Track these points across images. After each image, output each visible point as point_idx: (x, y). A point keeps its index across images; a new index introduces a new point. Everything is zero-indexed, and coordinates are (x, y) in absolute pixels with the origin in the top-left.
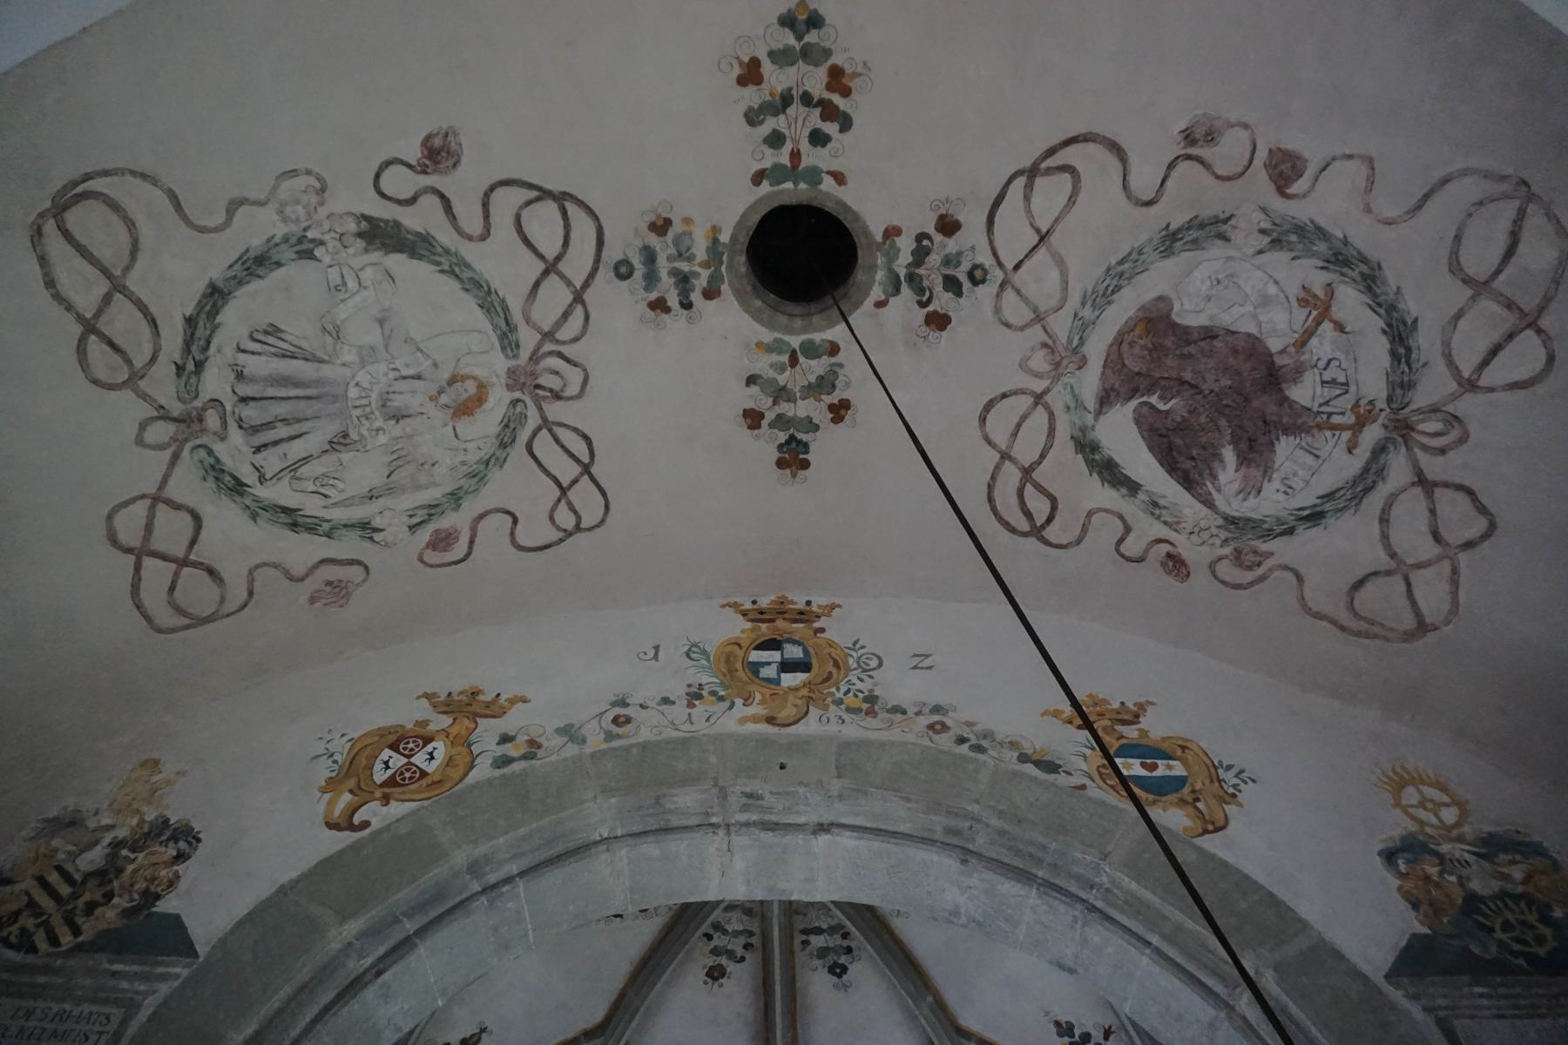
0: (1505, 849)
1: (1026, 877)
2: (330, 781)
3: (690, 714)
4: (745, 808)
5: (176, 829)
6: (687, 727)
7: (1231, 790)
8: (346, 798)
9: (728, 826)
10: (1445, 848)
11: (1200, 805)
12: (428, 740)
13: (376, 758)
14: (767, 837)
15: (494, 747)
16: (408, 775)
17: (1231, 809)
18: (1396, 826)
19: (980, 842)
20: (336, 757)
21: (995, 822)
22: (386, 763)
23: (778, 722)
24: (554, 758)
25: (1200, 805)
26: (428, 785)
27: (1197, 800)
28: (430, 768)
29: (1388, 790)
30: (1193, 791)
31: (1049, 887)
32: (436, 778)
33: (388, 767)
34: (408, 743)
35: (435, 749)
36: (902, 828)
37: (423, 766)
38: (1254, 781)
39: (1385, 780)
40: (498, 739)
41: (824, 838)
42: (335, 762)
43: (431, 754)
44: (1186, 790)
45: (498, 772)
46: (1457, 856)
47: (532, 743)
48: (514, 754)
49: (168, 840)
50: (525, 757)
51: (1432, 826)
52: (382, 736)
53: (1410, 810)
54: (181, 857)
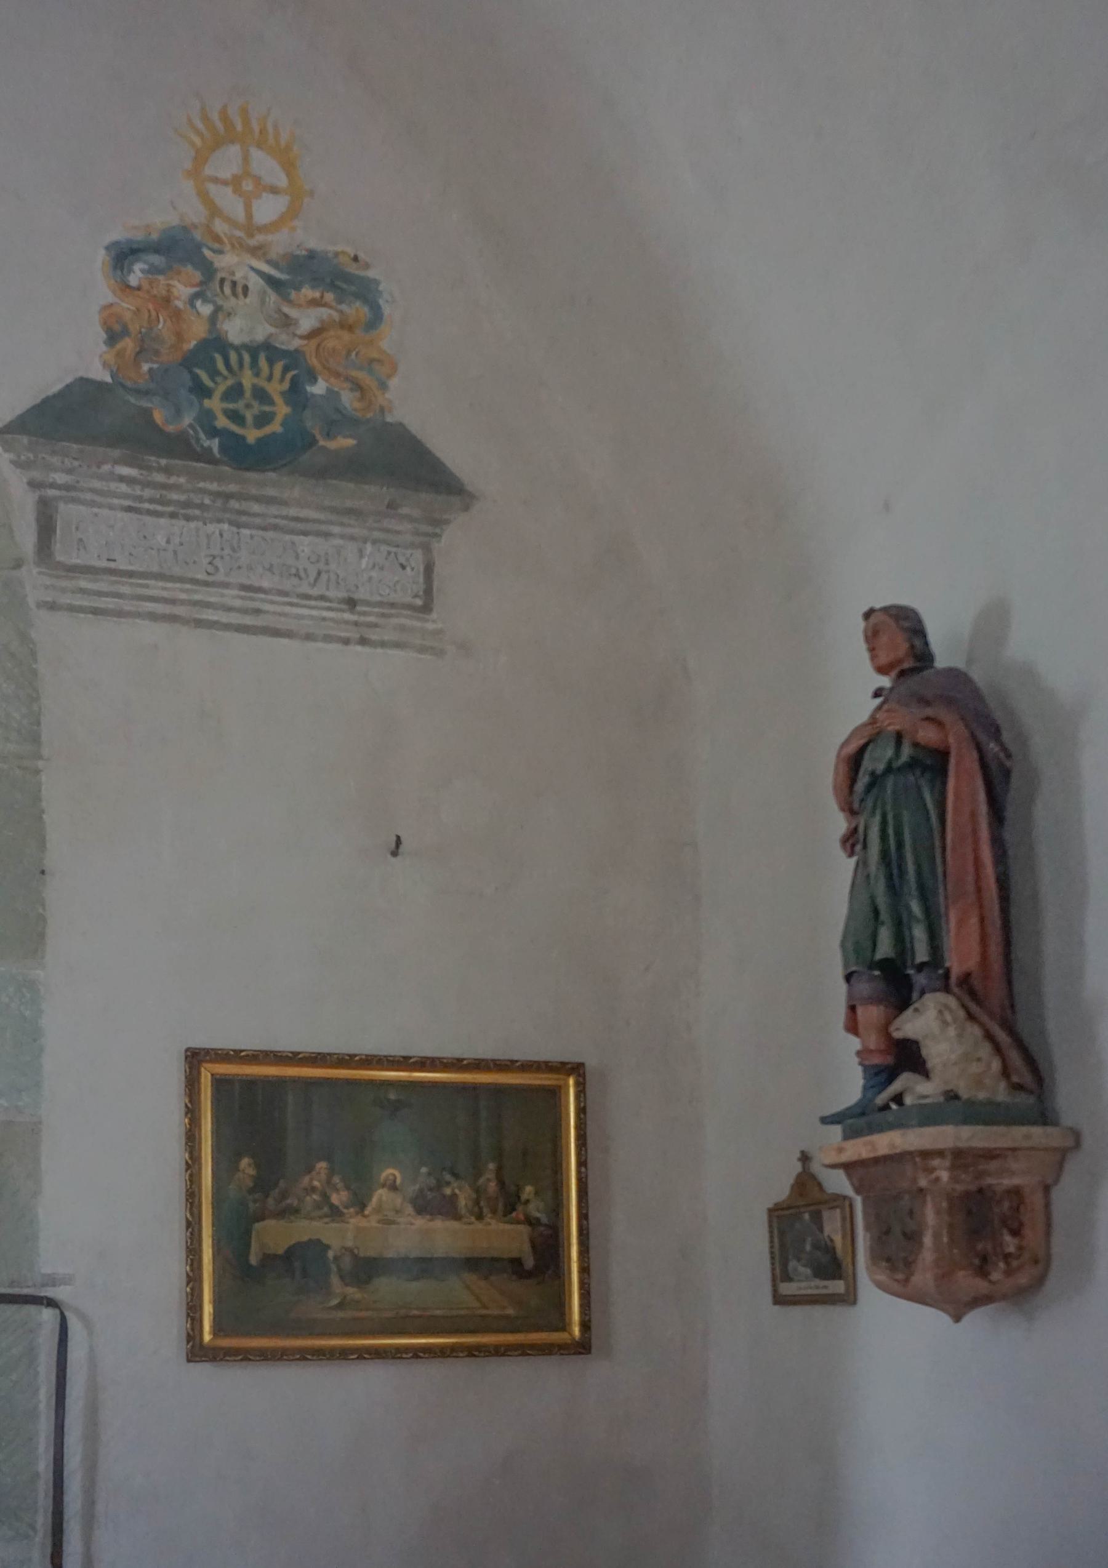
0: (316, 281)
10: (227, 261)
29: (193, 144)
39: (200, 125)
46: (238, 276)
51: (228, 220)
53: (212, 188)
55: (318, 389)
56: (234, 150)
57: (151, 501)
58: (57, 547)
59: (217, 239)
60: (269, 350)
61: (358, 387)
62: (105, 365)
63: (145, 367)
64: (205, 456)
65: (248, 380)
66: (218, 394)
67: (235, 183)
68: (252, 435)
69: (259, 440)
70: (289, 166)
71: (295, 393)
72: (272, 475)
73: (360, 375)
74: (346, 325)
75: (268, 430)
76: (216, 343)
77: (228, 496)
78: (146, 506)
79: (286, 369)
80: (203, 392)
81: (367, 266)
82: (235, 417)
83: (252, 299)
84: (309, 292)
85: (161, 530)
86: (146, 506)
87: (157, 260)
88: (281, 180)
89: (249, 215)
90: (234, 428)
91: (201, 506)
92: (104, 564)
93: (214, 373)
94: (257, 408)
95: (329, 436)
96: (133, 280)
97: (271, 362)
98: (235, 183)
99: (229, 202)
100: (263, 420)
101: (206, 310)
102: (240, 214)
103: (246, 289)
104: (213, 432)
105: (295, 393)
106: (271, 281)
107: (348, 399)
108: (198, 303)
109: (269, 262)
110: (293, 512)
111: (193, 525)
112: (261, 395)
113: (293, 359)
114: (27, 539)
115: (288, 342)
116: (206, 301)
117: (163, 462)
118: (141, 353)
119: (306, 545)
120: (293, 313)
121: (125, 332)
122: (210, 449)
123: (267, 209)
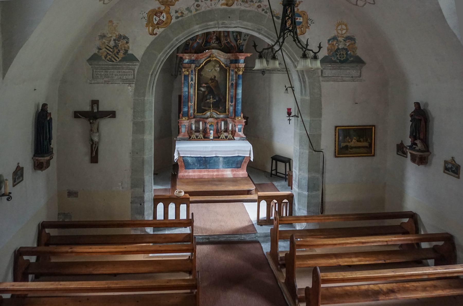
2: (146, 24)
3: (211, 3)
5: (123, 37)
6: (211, 7)
7: (309, 25)
8: (151, 28)
11: (302, 29)
12: (162, 13)
13: (153, 18)
15: (175, 14)
17: (307, 30)
18: (334, 33)
19: (262, 32)
21: (266, 29)
22: (155, 19)
23: (228, 5)
24: (187, 16)
25: (302, 29)
26: (165, 24)
27: (302, 27)
28: (164, 20)
30: (302, 25)
34: (158, 14)
35: (164, 15)
36: (250, 28)
37: (162, 19)
38: (314, 23)
40: (175, 12)
43: (163, 16)
44: (301, 25)
45: (177, 20)
47: (182, 13)
48: (179, 15)
49: (123, 39)
52: (152, 12)
54: (127, 43)
55: (349, 53)
57: (332, 68)
58: (323, 74)
59: (338, 36)
60: (343, 49)
61: (353, 51)
62: (327, 54)
63: (331, 53)
64: (337, 63)
65: (342, 53)
66: (338, 55)
67: (340, 30)
68: (342, 59)
69: (343, 60)
70: (346, 26)
71: (347, 54)
72: (344, 64)
73: (353, 50)
74: (352, 44)
75: (343, 59)
76: (338, 49)
77: (340, 67)
78: (332, 69)
79: (346, 51)
80: (337, 55)
81: (354, 37)
82: (340, 57)
83: (342, 43)
84: (348, 41)
85: (334, 71)
86: (332, 69)
87: (332, 40)
88: (345, 28)
89: (342, 33)
90: (341, 59)
91: (337, 68)
92: (328, 76)
93: (338, 52)
94: (343, 56)
95: (350, 58)
96: (330, 43)
97: (344, 50)
98: (340, 30)
99: (340, 32)
100: (343, 57)
101: (337, 45)
102: (341, 33)
103: (341, 41)
104: (338, 60)
105: (347, 54)
106: (344, 40)
107: (352, 53)
108: (336, 44)
109: (344, 38)
110: (346, 68)
111: (336, 70)
112: (343, 54)
113: (346, 49)
114: (320, 74)
115: (346, 47)
116: (337, 44)
117: (333, 64)
118: (331, 51)
119: (348, 71)
121: (329, 49)
122: (338, 62)
123: (344, 32)
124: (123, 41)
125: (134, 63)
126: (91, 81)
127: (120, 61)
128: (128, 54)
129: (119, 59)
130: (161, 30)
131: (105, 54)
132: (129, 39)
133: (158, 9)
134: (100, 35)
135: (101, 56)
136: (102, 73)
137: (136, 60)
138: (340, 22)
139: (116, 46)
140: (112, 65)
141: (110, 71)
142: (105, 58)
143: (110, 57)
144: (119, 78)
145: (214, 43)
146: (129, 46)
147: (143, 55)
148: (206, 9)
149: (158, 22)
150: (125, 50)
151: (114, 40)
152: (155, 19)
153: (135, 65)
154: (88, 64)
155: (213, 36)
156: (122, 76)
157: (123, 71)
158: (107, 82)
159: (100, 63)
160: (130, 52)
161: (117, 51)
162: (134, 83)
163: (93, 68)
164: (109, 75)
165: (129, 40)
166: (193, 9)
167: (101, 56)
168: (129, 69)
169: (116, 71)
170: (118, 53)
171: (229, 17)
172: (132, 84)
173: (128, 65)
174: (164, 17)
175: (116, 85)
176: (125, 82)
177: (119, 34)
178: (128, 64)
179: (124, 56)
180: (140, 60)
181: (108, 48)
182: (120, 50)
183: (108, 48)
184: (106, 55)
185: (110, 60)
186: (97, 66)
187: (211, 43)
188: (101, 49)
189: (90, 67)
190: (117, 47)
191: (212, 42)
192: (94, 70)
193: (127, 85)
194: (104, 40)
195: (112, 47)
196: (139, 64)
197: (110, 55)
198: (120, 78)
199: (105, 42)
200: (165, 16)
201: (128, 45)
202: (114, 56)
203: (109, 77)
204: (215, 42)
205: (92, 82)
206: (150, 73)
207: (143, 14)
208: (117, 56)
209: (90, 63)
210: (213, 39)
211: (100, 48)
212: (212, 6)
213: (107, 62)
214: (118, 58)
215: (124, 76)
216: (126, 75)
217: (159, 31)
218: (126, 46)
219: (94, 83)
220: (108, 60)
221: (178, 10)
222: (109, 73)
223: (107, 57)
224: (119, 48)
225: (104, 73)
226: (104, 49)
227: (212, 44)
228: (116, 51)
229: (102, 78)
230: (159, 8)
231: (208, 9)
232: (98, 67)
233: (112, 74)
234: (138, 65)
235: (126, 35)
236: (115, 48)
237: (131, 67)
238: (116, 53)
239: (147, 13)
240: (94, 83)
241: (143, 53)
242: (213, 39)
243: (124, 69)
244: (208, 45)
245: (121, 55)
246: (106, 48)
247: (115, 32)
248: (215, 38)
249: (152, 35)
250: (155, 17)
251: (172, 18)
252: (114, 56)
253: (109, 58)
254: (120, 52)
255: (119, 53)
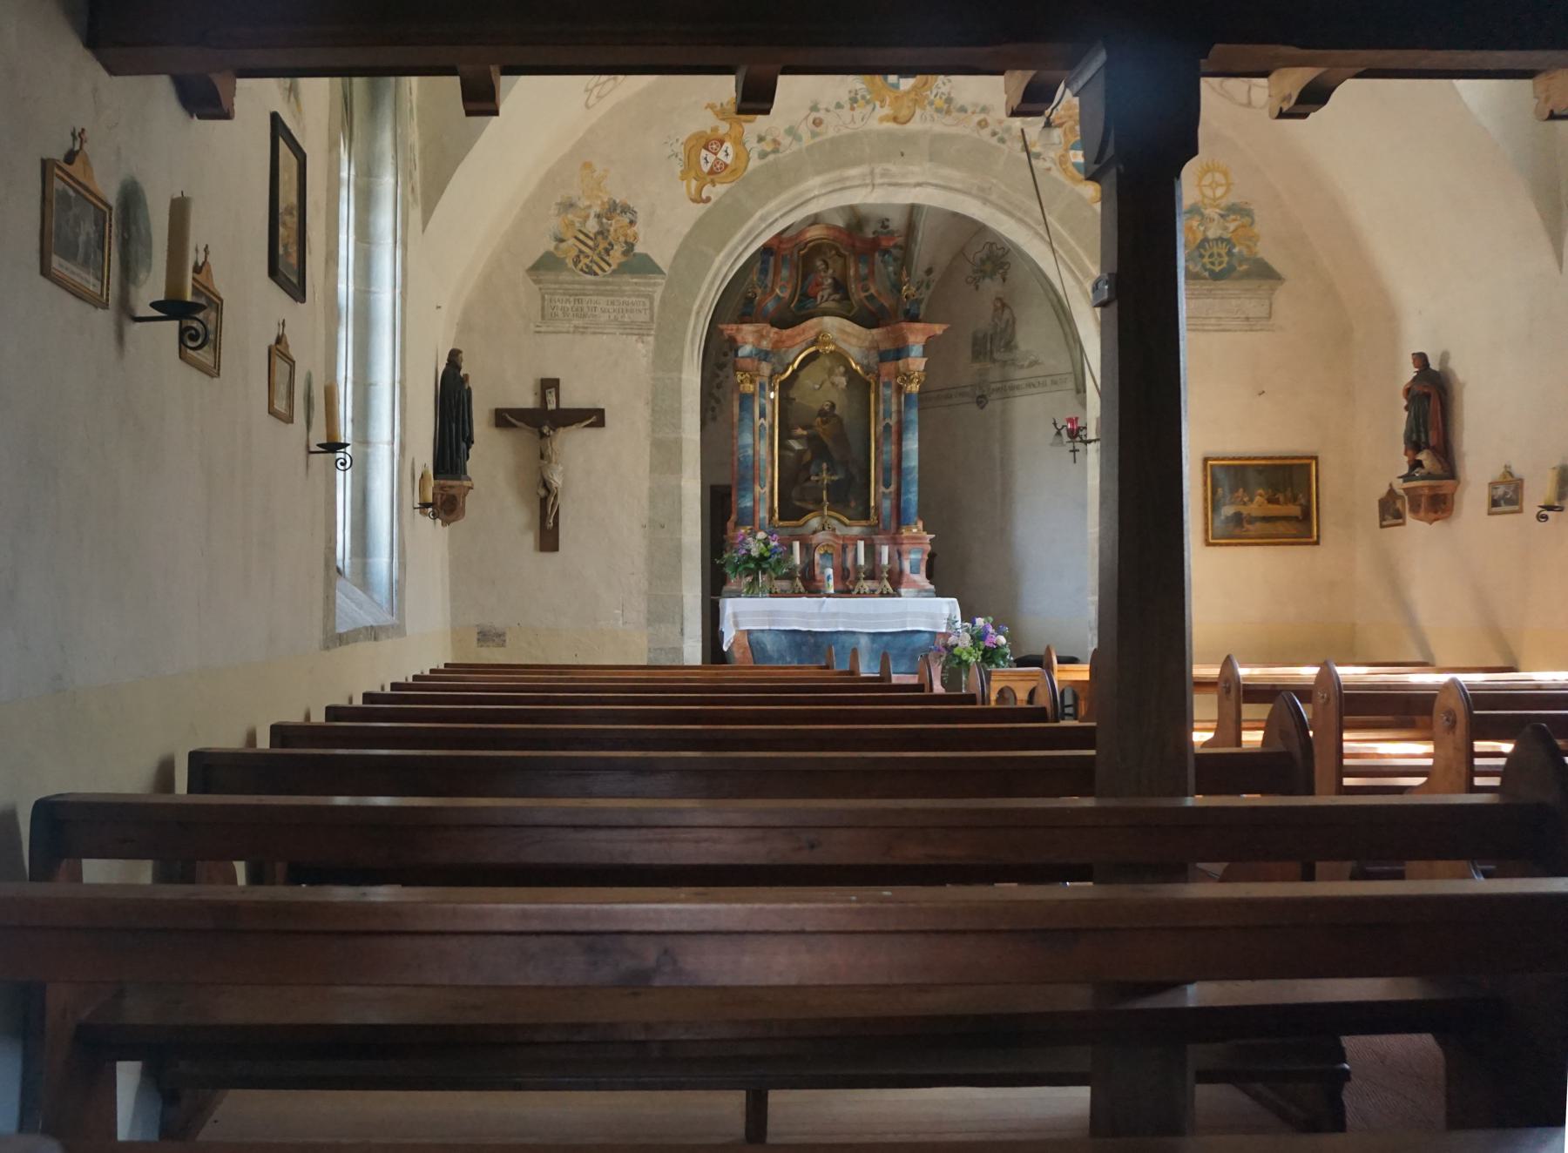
1: (1010, 214)
2: (682, 172)
4: (883, 175)
8: (694, 183)
9: (873, 185)
12: (722, 142)
14: (891, 188)
16: (718, 166)
19: (993, 197)
20: (680, 156)
21: (1003, 188)
24: (788, 152)
28: (729, 160)
31: (1020, 221)
32: (733, 168)
33: (707, 162)
41: (918, 189)
42: (680, 160)
43: (726, 151)
45: (763, 162)
47: (775, 141)
48: (769, 149)
50: (775, 151)
56: (1209, 175)
59: (1205, 205)
74: (1243, 226)
83: (1216, 222)
84: (1232, 217)
87: (1188, 215)
88: (1223, 182)
89: (1214, 195)
98: (1210, 185)
99: (1208, 192)
106: (1222, 216)
109: (1222, 209)
120: (1227, 225)
123: (1219, 192)
124: (621, 218)
125: (650, 278)
126: (538, 326)
127: (614, 272)
128: (635, 255)
129: (612, 268)
130: (721, 189)
131: (574, 253)
132: (635, 212)
133: (712, 130)
134: (559, 201)
135: (565, 258)
136: (568, 305)
137: (656, 270)
138: (1207, 165)
139: (602, 233)
140: (595, 283)
141: (588, 298)
142: (576, 264)
143: (587, 261)
144: (612, 317)
145: (827, 300)
146: (636, 233)
147: (675, 258)
148: (839, 130)
149: (712, 168)
150: (626, 242)
151: (598, 216)
152: (706, 159)
153: (655, 284)
154: (529, 279)
155: (822, 277)
156: (621, 314)
157: (622, 300)
158: (581, 331)
159: (561, 278)
160: (639, 249)
161: (606, 245)
162: (653, 332)
163: (543, 291)
164: (586, 310)
165: (636, 218)
166: (804, 130)
167: (565, 258)
168: (638, 296)
169: (603, 299)
170: (607, 252)
171: (902, 155)
172: (648, 335)
173: (636, 283)
174: (727, 153)
175: (605, 337)
176: (629, 331)
177: (610, 199)
178: (635, 280)
179: (623, 259)
180: (666, 271)
181: (581, 237)
182: (613, 242)
183: (581, 237)
184: (578, 256)
185: (587, 270)
186: (553, 286)
187: (819, 298)
188: (562, 241)
189: (536, 287)
190: (606, 234)
191: (823, 297)
192: (546, 296)
193: (635, 338)
194: (570, 216)
195: (592, 235)
196: (663, 281)
197: (587, 256)
198: (616, 319)
199: (573, 221)
200: (730, 151)
201: (635, 228)
202: (596, 258)
203: (585, 316)
204: (832, 297)
205: (542, 329)
206: (695, 307)
207: (671, 145)
208: (607, 258)
209: (535, 278)
210: (824, 287)
211: (560, 236)
212: (855, 123)
213: (579, 275)
214: (609, 265)
215: (626, 315)
216: (632, 311)
217: (715, 191)
218: (629, 231)
219: (545, 332)
220: (582, 270)
221: (763, 134)
222: (585, 305)
223: (580, 261)
224: (610, 237)
225: (572, 304)
226: (573, 241)
227: (821, 303)
228: (603, 245)
229: (566, 317)
230: (715, 129)
231: (845, 131)
232: (555, 289)
233: (595, 307)
234: (661, 284)
235: (628, 203)
236: (599, 237)
237: (643, 289)
238: (603, 251)
239: (682, 144)
240: (545, 332)
241: (674, 252)
242: (824, 287)
243: (626, 296)
244: (809, 305)
245: (616, 256)
246: (576, 238)
247: (600, 194)
248: (830, 284)
249: (699, 202)
250: (704, 153)
251: (751, 155)
252: (596, 258)
253: (586, 264)
254: (612, 249)
255: (611, 252)
